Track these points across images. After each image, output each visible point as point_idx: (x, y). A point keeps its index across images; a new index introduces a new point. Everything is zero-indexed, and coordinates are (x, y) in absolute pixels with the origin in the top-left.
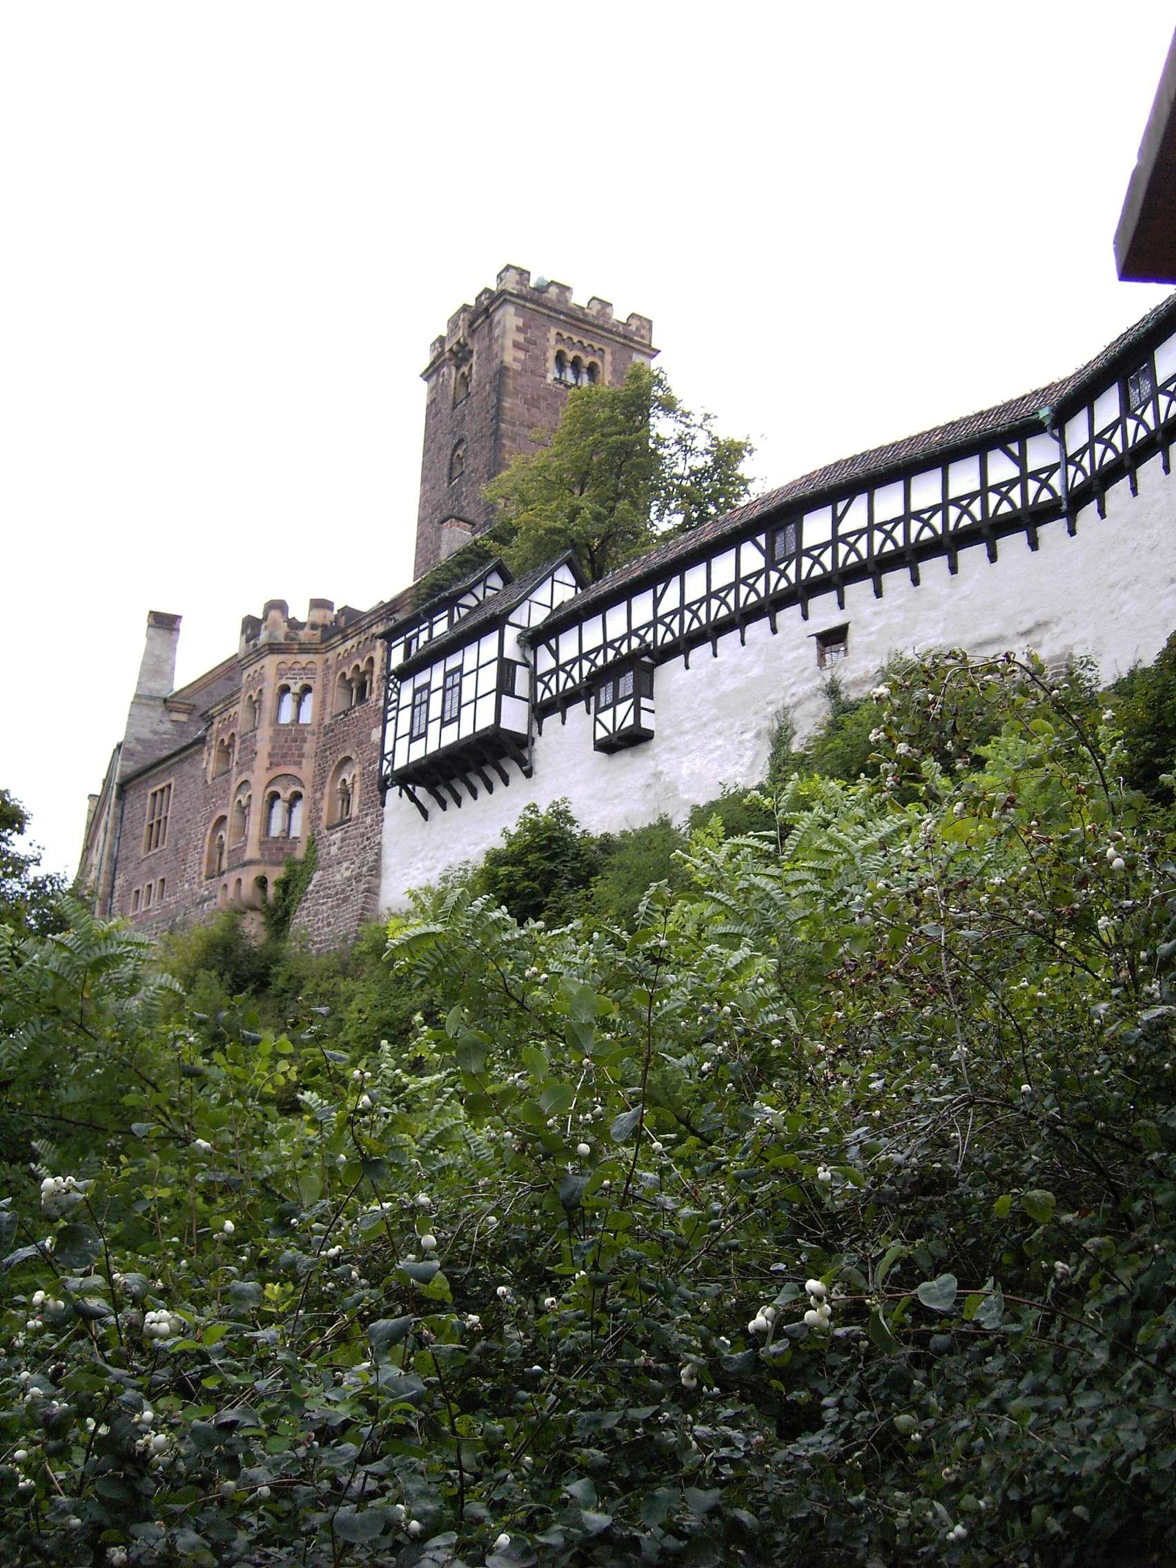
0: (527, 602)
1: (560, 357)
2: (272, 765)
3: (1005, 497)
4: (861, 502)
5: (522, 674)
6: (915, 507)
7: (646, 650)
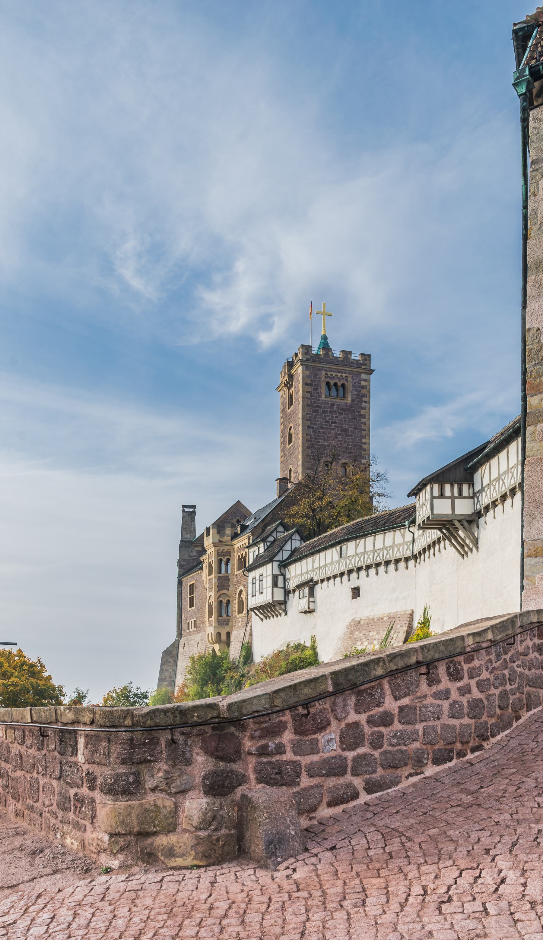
0: (281, 551)
1: (328, 384)
2: (219, 590)
3: (399, 550)
4: (363, 540)
5: (281, 578)
6: (376, 548)
7: (311, 580)
